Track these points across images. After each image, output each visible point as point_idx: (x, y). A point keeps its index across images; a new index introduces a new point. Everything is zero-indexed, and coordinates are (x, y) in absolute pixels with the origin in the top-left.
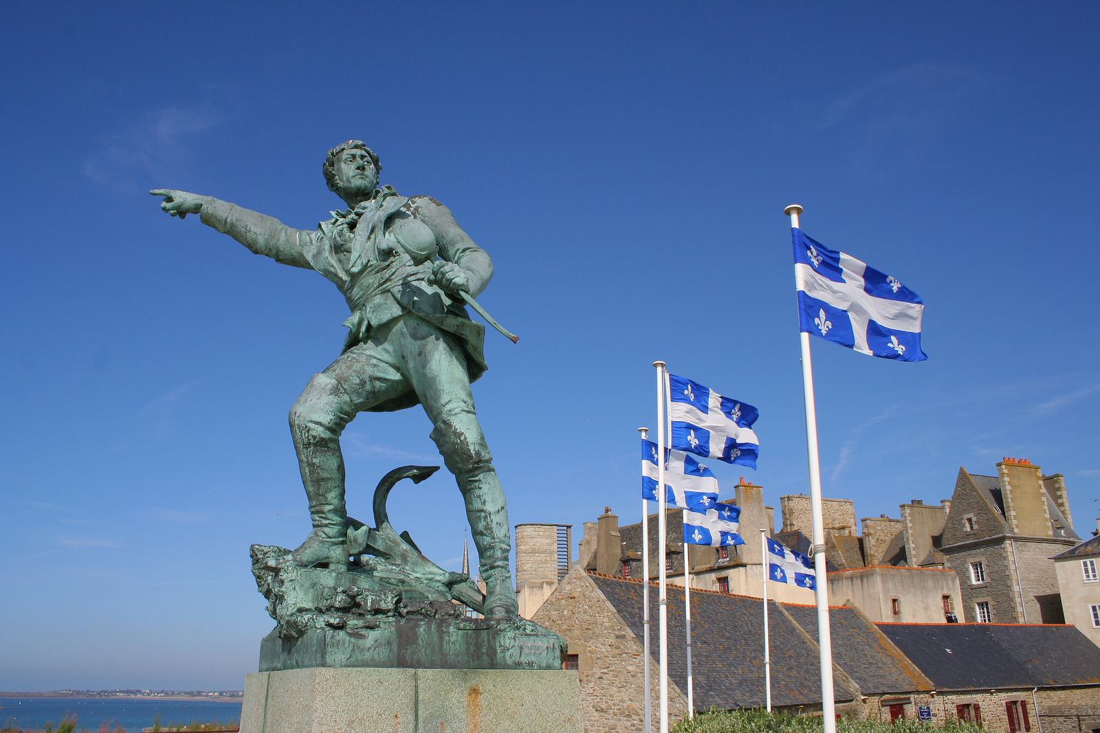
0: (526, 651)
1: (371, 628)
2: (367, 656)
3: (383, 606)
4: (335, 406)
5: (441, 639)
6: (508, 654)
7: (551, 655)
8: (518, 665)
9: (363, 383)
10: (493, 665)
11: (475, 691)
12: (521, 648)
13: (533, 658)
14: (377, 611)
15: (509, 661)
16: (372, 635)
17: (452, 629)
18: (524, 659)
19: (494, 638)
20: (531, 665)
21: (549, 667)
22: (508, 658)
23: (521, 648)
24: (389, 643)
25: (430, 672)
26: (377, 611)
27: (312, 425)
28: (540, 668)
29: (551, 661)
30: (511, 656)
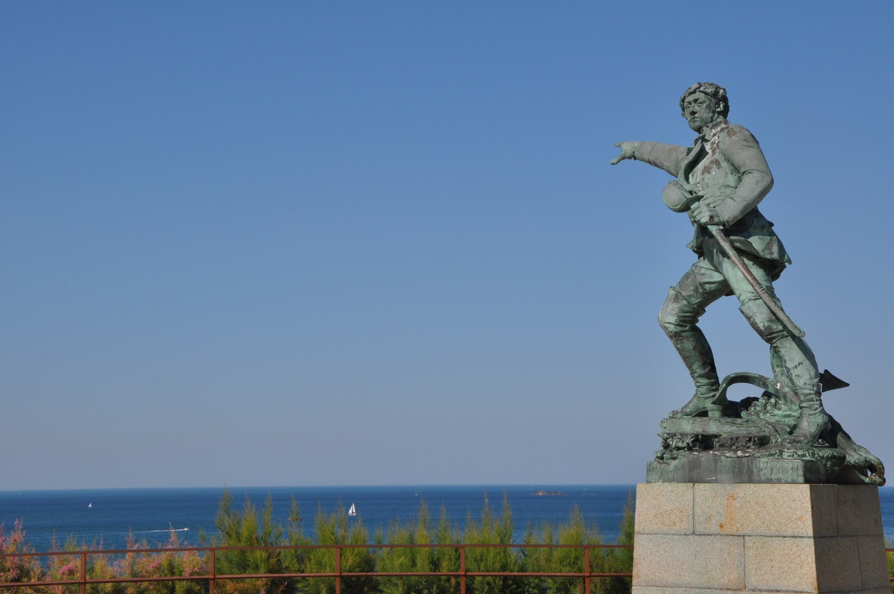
0: (775, 471)
1: (674, 459)
2: (670, 476)
3: (680, 445)
4: (677, 310)
5: (716, 464)
6: (762, 473)
7: (795, 474)
8: (769, 481)
9: (696, 290)
10: (750, 481)
11: (732, 497)
12: (772, 469)
13: (781, 476)
14: (678, 449)
15: (763, 478)
16: (674, 463)
17: (723, 458)
18: (774, 477)
19: (752, 462)
20: (779, 481)
21: (794, 482)
22: (762, 475)
23: (772, 469)
24: (683, 467)
25: (702, 485)
26: (678, 449)
27: (667, 325)
28: (787, 483)
29: (795, 478)
30: (765, 474)
